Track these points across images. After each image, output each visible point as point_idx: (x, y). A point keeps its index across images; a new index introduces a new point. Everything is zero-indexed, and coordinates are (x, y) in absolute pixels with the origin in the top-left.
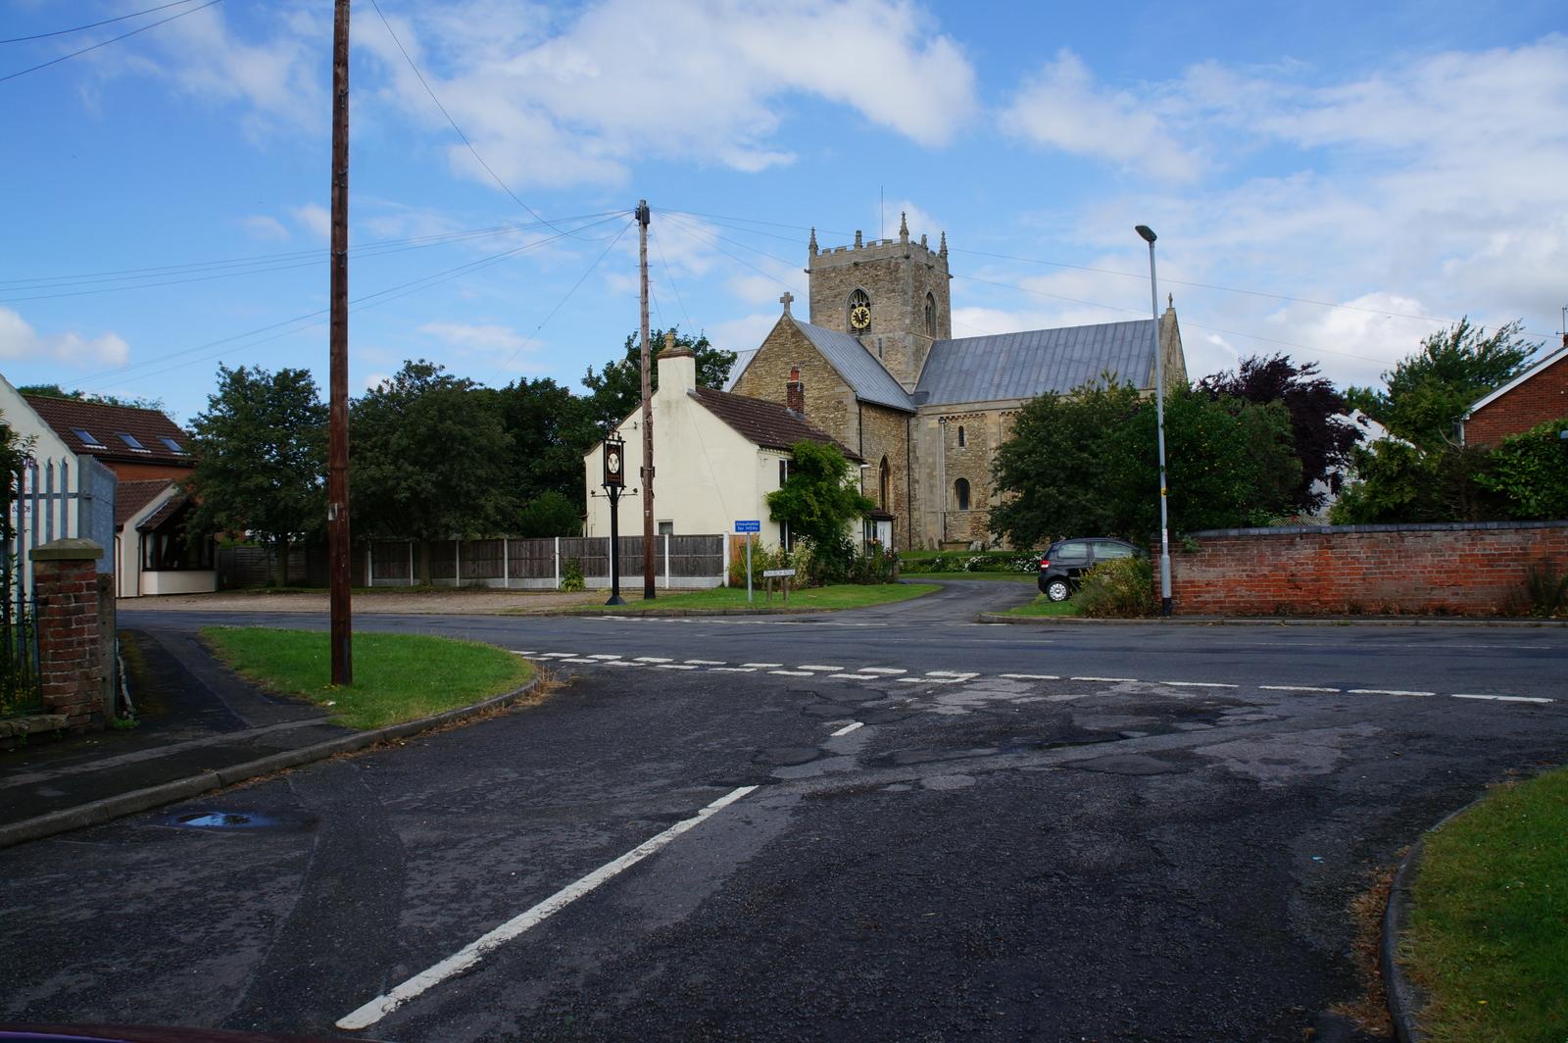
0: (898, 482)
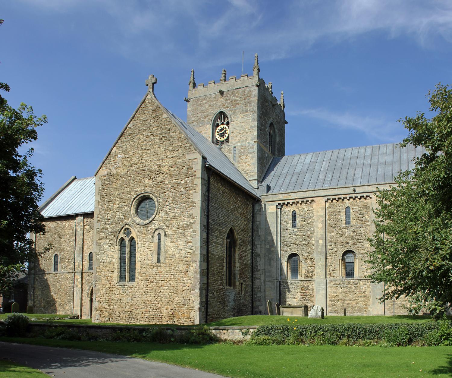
0: (243, 254)
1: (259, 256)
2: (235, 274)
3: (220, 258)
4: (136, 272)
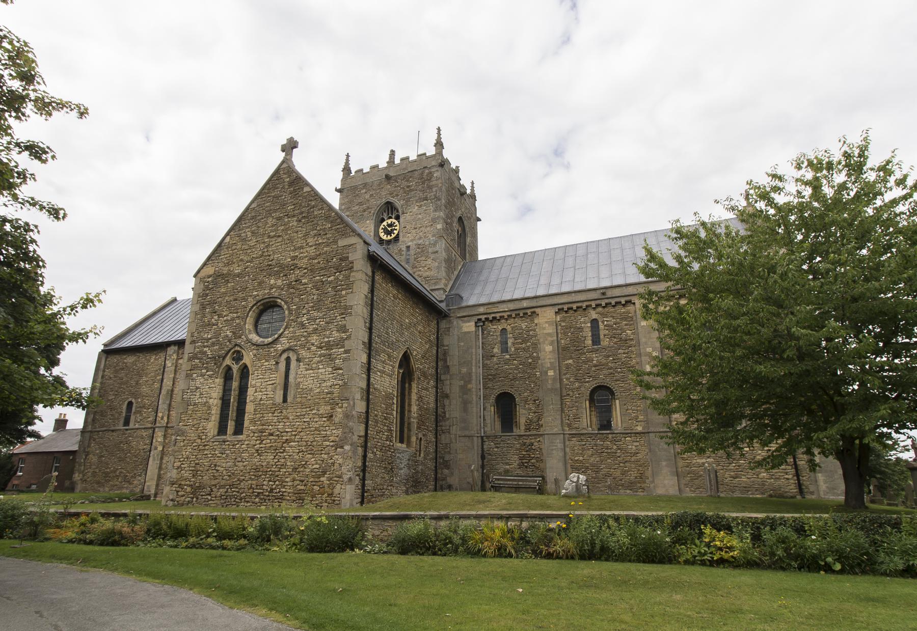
2: (409, 424)
4: (246, 418)
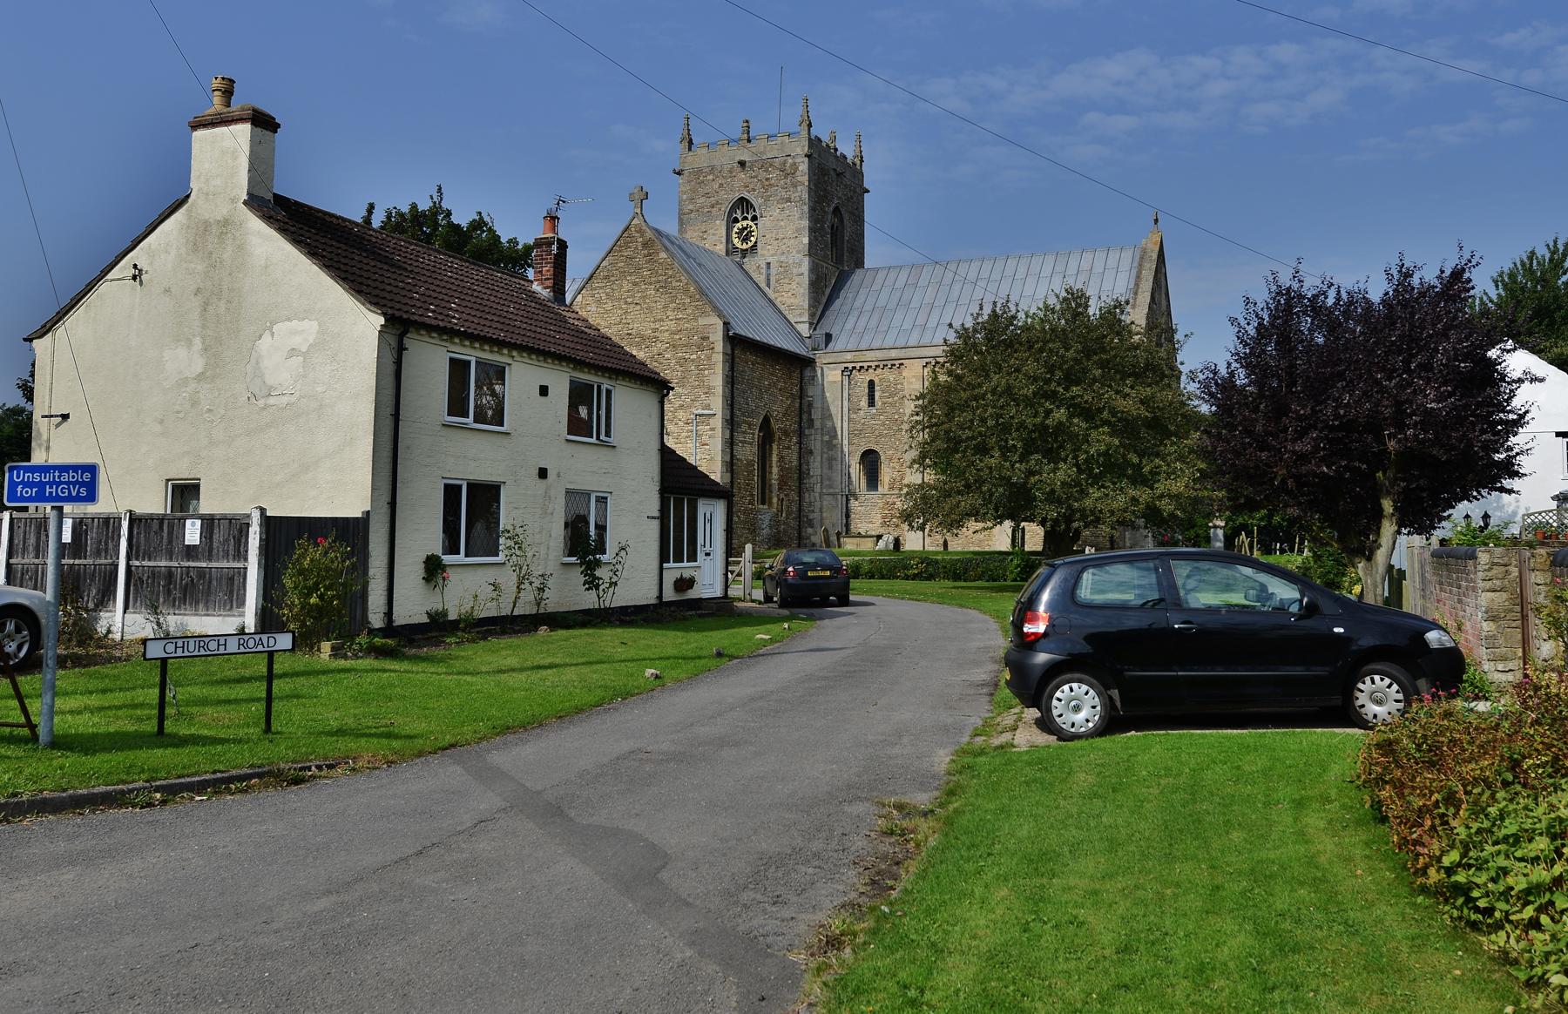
1: (811, 452)
3: (750, 464)
